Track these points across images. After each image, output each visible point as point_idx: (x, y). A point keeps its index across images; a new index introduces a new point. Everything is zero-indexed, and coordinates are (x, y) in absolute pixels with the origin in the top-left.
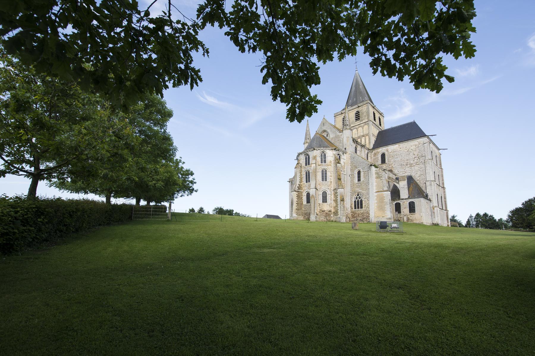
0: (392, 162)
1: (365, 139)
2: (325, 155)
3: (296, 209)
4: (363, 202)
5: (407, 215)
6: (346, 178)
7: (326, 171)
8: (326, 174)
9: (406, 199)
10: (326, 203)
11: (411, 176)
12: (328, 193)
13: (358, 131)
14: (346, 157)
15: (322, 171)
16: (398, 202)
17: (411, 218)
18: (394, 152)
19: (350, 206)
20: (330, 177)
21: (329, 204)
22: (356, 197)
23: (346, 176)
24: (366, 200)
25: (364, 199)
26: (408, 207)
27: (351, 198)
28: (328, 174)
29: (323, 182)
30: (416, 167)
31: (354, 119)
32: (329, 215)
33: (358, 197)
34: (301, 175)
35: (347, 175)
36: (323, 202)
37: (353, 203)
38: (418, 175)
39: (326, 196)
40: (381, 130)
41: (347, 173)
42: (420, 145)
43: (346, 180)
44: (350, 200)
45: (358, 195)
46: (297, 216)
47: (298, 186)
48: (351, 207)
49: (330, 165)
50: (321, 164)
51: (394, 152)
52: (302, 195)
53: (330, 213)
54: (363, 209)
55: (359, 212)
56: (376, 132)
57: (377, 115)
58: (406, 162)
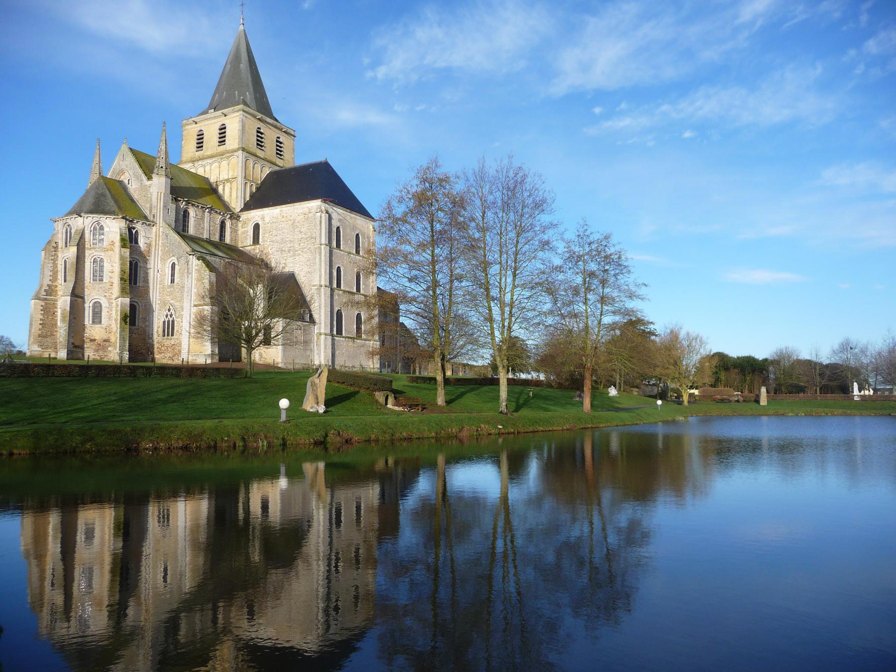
0: (268, 243)
1: (231, 188)
3: (39, 336)
10: (99, 326)
11: (293, 274)
12: (104, 303)
18: (273, 222)
20: (110, 274)
21: (105, 327)
24: (180, 320)
28: (107, 266)
31: (216, 139)
32: (104, 348)
34: (55, 265)
36: (94, 322)
39: (101, 311)
40: (277, 168)
42: (310, 215)
46: (40, 349)
49: (112, 250)
51: (273, 222)
53: (107, 344)
54: (175, 337)
55: (168, 343)
56: (262, 172)
57: (270, 135)
58: (289, 245)
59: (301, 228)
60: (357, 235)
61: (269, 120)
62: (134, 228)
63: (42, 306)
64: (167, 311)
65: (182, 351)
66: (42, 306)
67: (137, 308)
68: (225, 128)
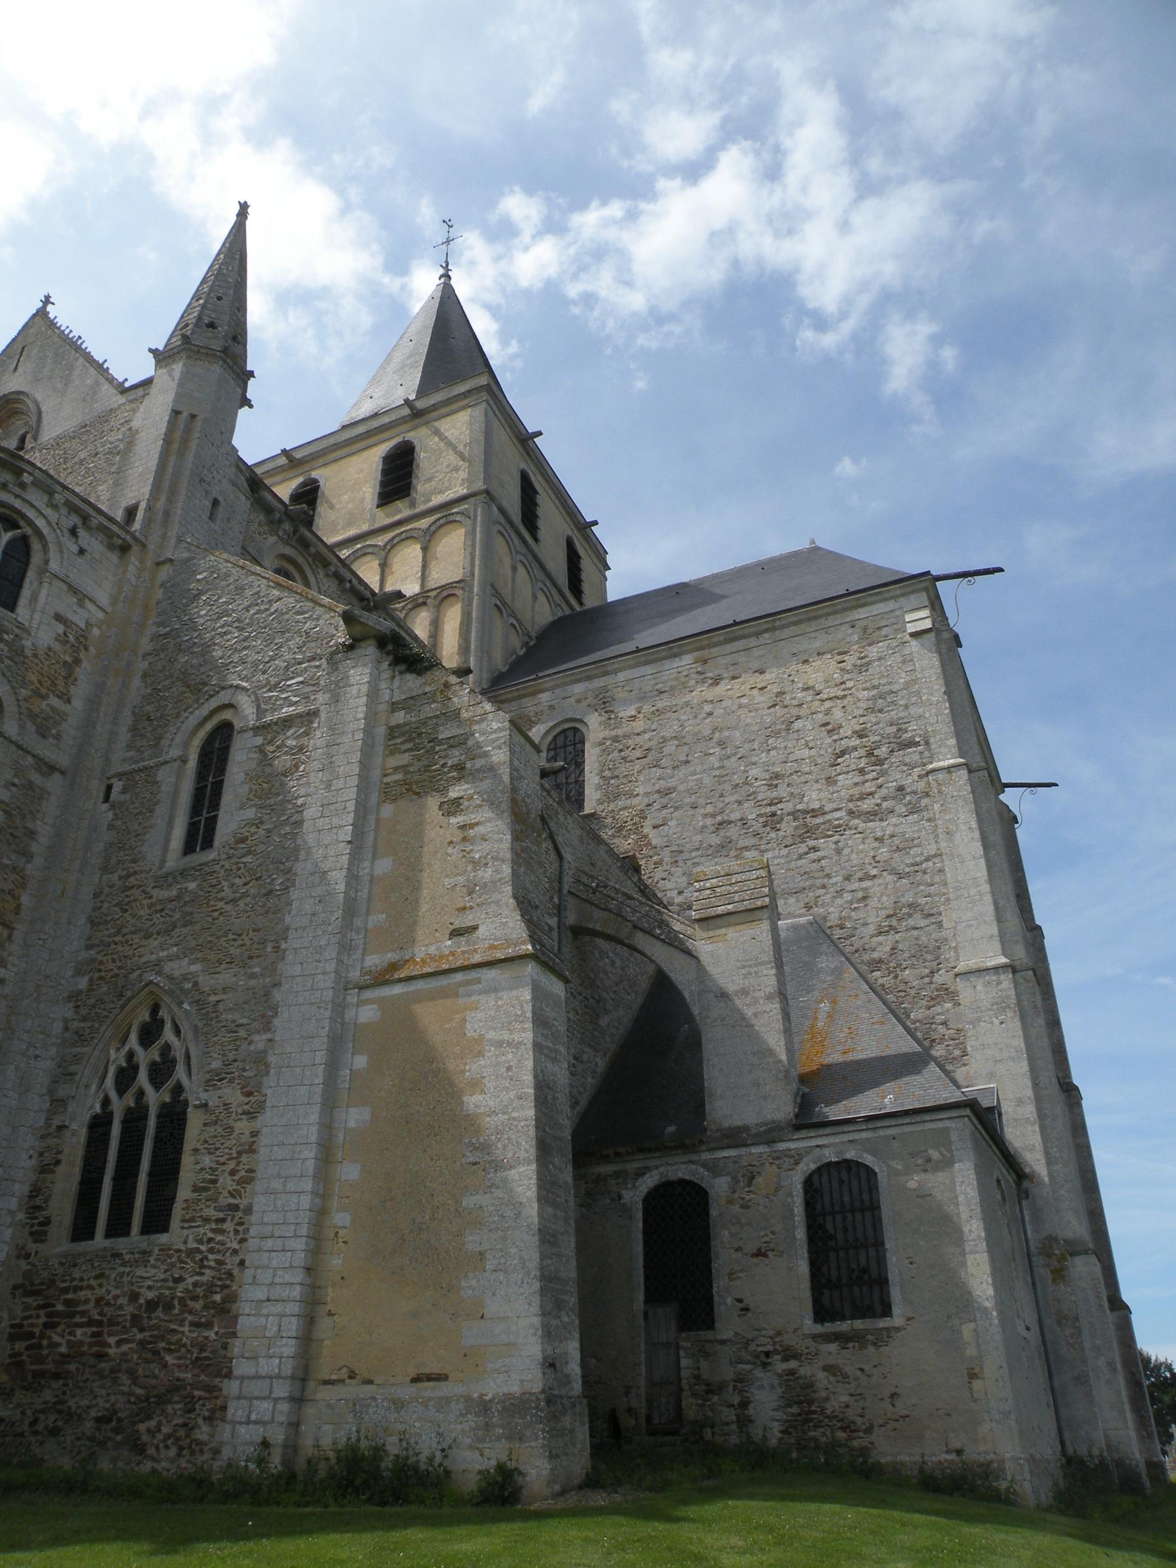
4: (195, 1123)
5: (789, 1354)
9: (771, 1134)
16: (680, 1168)
17: (839, 1399)
19: (21, 1189)
22: (117, 1058)
23: (55, 784)
25: (215, 1080)
26: (801, 1234)
27: (65, 1073)
30: (850, 840)
31: (369, 491)
33: (144, 1058)
38: (873, 916)
43: (44, 830)
45: (149, 1034)
54: (177, 1236)
58: (764, 794)
59: (828, 712)
64: (133, 1041)
65: (241, 1367)
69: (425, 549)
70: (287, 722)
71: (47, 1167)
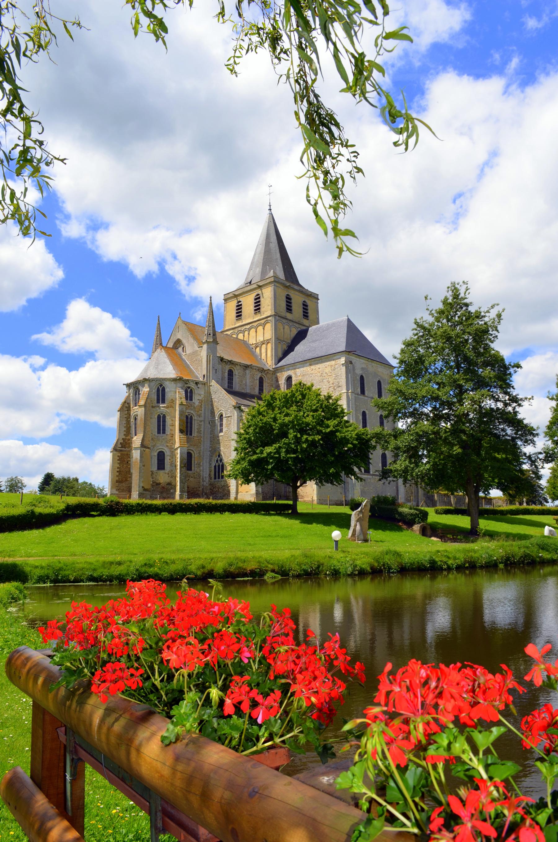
2: (164, 389)
3: (117, 482)
6: (202, 426)
7: (164, 417)
8: (164, 421)
13: (256, 332)
14: (205, 390)
15: (159, 417)
19: (208, 474)
22: (216, 459)
27: (210, 460)
29: (159, 435)
35: (204, 421)
37: (213, 469)
41: (205, 418)
43: (202, 429)
44: (208, 464)
47: (122, 441)
48: (210, 475)
50: (157, 405)
51: (303, 375)
52: (130, 457)
53: (170, 487)
57: (297, 300)
60: (379, 383)
61: (296, 287)
62: (189, 388)
63: (118, 456)
66: (118, 456)
67: (193, 455)
68: (259, 298)
69: (264, 329)
70: (229, 417)
71: (210, 471)
